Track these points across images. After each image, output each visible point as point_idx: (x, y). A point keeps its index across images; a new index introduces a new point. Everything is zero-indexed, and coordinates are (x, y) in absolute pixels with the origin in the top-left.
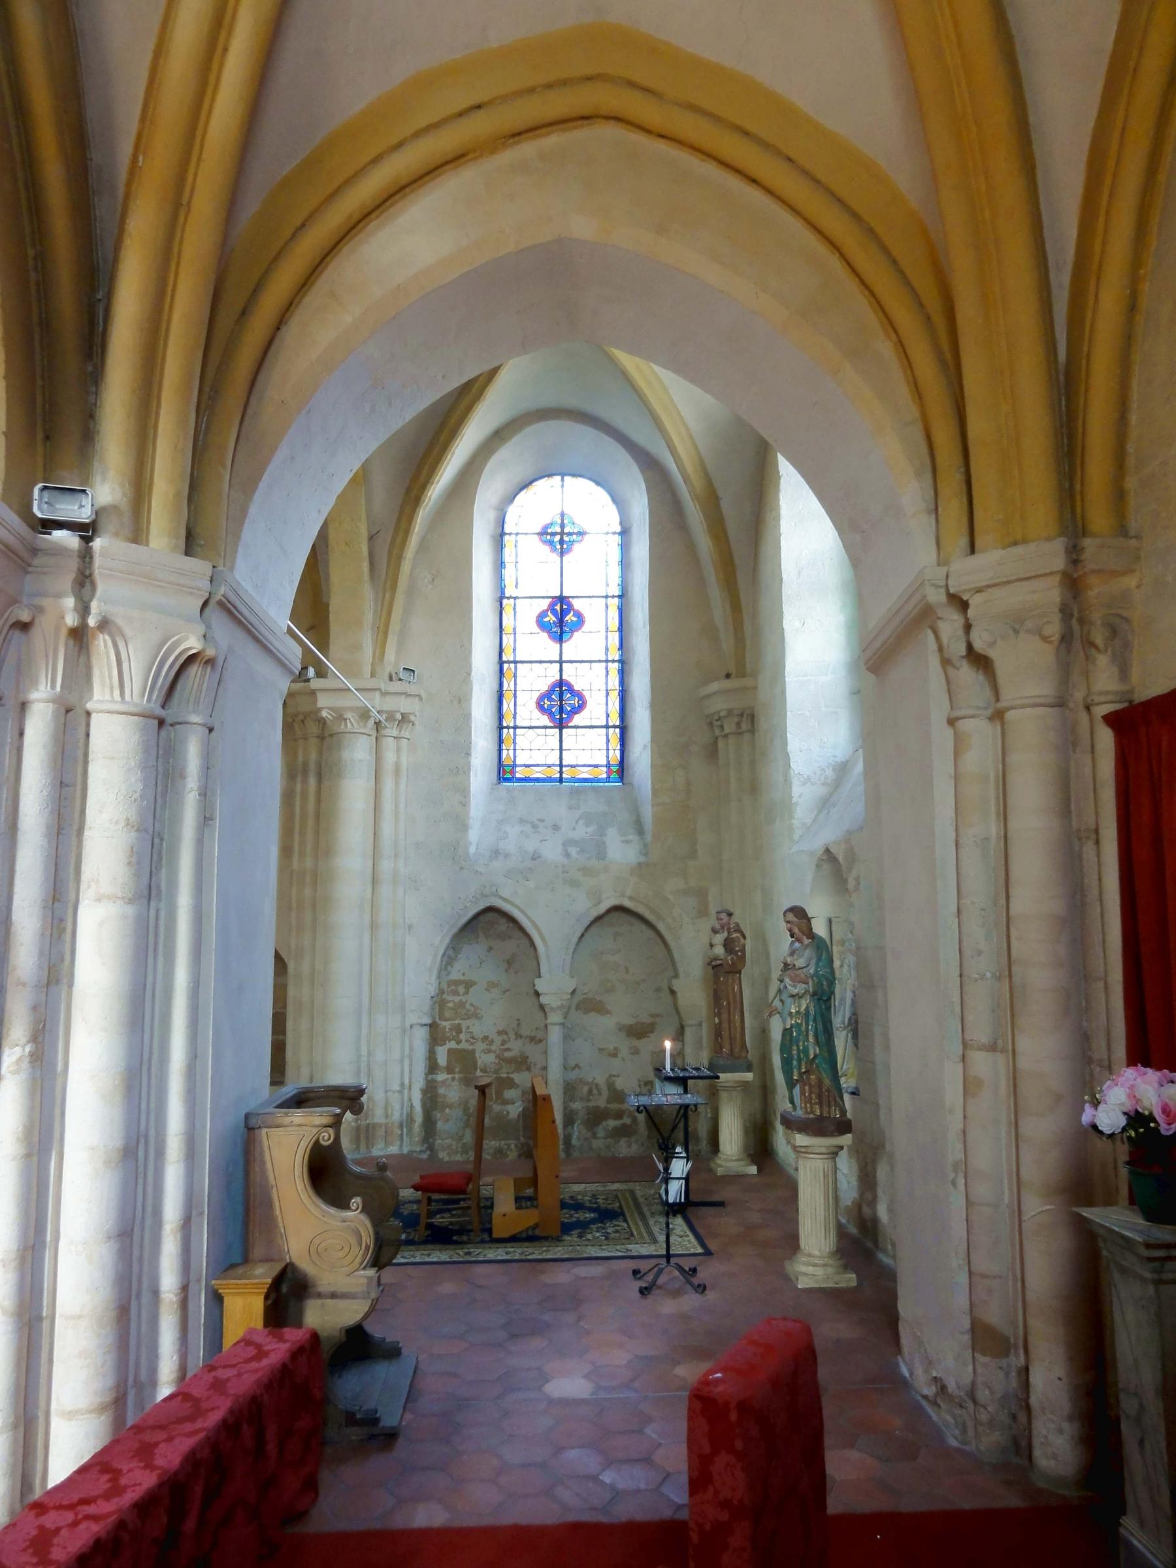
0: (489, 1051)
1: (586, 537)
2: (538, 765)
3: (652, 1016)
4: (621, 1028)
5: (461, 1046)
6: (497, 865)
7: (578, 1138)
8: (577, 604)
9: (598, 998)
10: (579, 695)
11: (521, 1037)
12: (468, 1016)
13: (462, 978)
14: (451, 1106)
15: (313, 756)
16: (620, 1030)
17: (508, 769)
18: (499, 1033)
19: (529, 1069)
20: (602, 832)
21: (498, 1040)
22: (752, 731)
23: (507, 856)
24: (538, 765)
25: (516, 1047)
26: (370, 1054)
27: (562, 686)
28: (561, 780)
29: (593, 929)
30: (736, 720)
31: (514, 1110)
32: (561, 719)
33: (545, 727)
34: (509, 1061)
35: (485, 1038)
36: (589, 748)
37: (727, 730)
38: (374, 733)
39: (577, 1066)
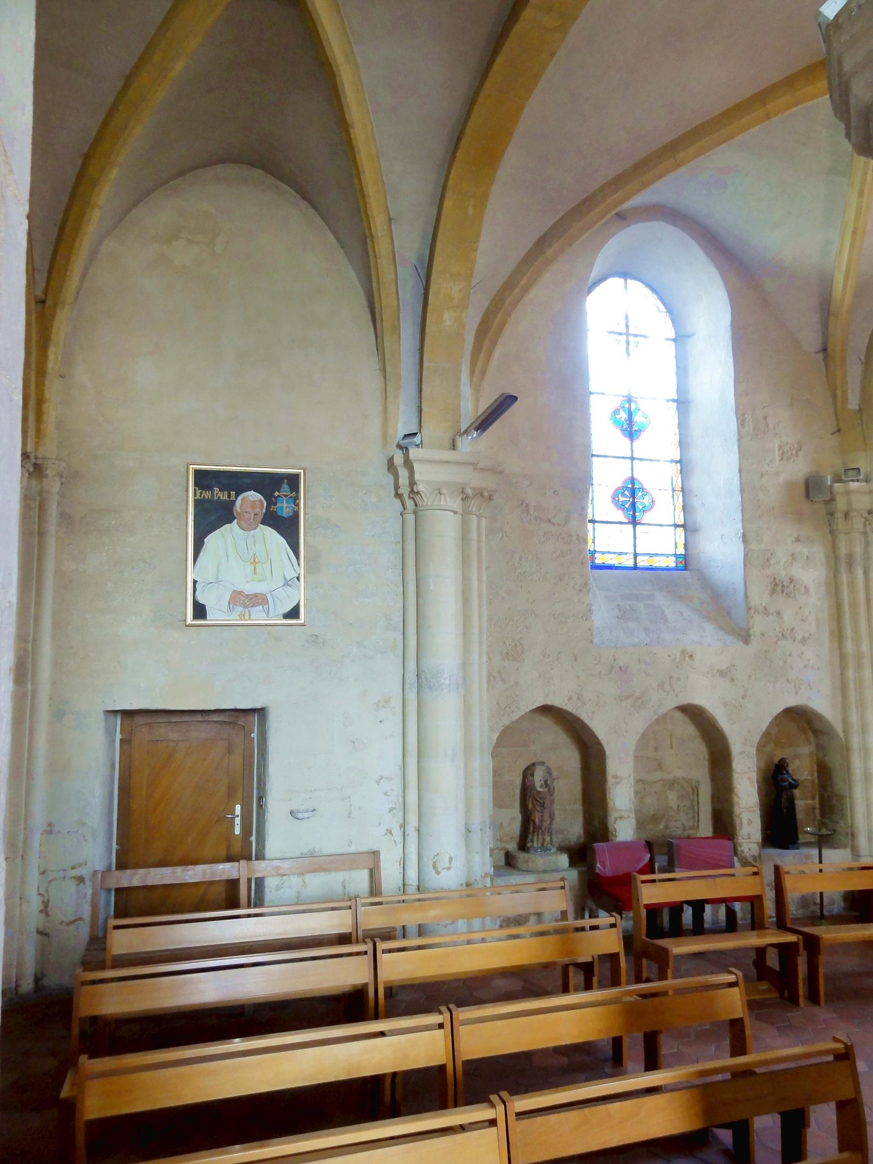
15: (858, 550)
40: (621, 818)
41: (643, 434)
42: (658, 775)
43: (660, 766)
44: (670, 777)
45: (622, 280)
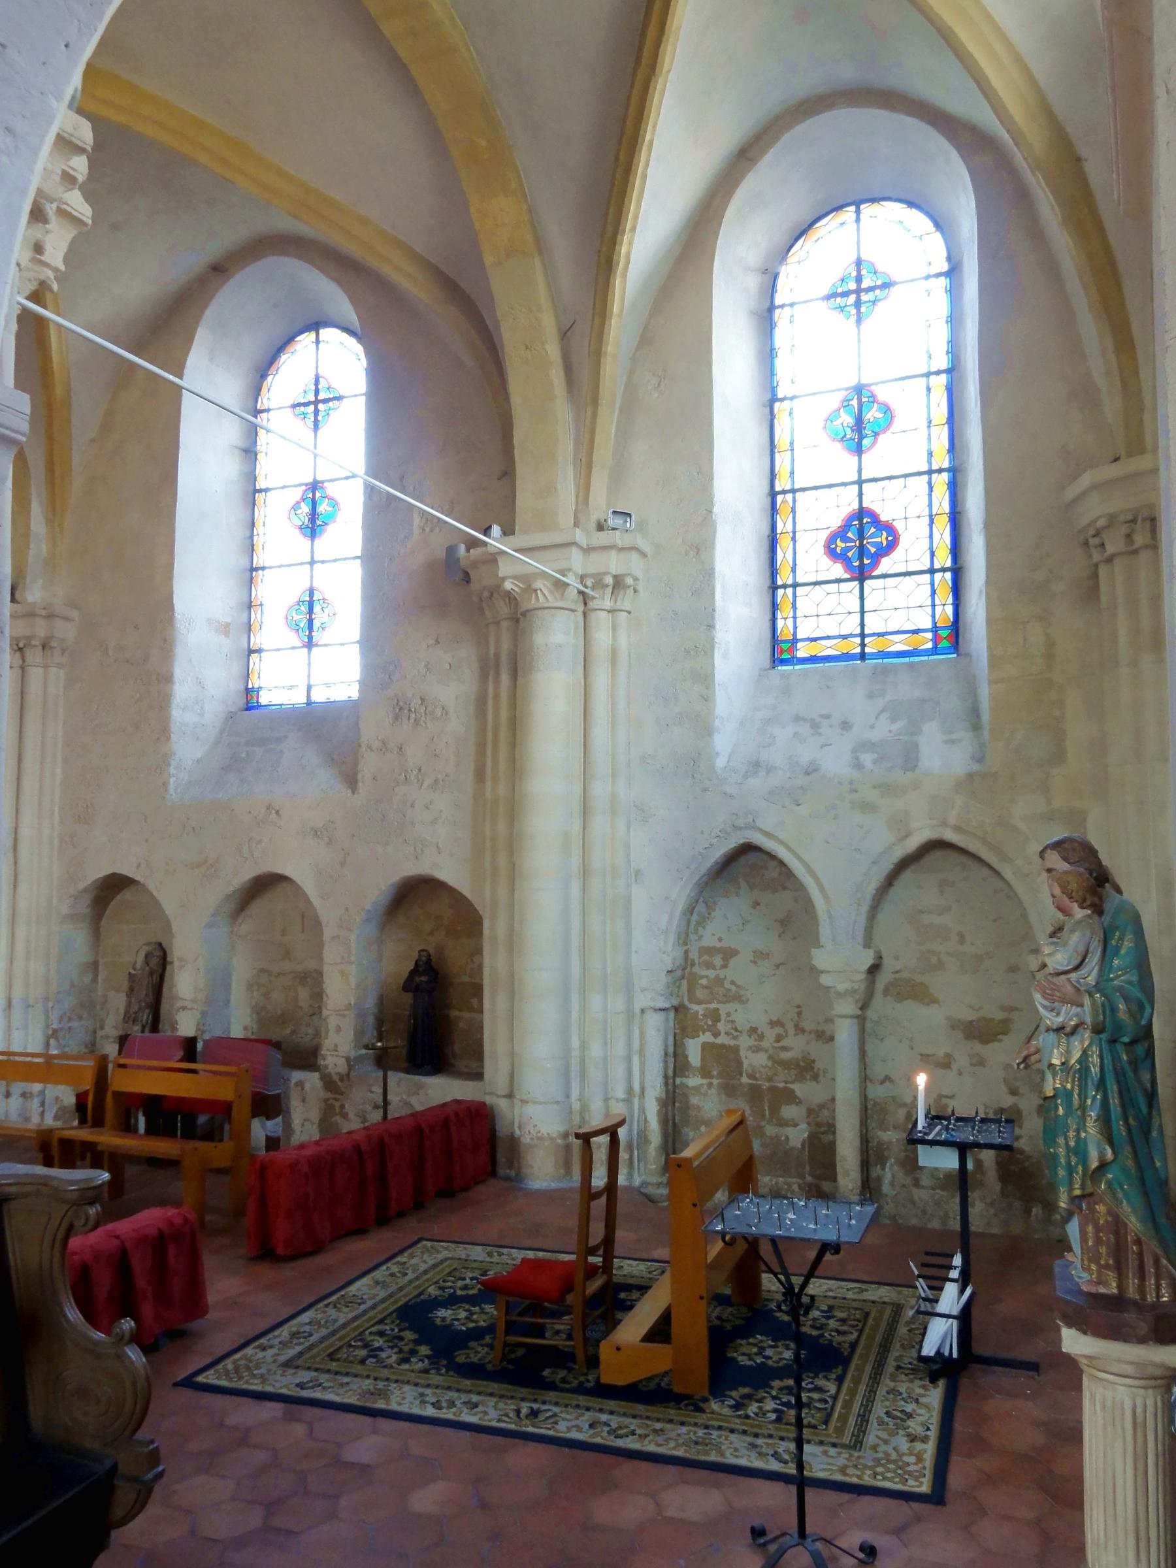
0: (758, 1049)
1: (894, 290)
2: (828, 638)
3: (1003, 1008)
4: (954, 1025)
5: (719, 1041)
6: (755, 783)
7: (892, 1184)
8: (882, 394)
9: (919, 978)
10: (889, 528)
11: (803, 1031)
12: (729, 998)
13: (719, 945)
14: (708, 1123)
15: (505, 645)
16: (953, 1027)
17: (785, 646)
18: (773, 1024)
19: (815, 1078)
20: (914, 728)
21: (771, 1034)
22: (1154, 546)
23: (770, 770)
24: (828, 638)
25: (796, 1046)
26: (583, 1046)
27: (863, 518)
28: (863, 656)
29: (907, 875)
30: (1124, 529)
31: (797, 1136)
32: (862, 564)
33: (838, 581)
34: (786, 1064)
35: (753, 1030)
36: (904, 605)
37: (1110, 549)
38: (581, 608)
39: (887, 1079)
40: (184, 1008)
41: (330, 528)
42: (288, 966)
43: (288, 955)
44: (299, 968)
45: (313, 335)
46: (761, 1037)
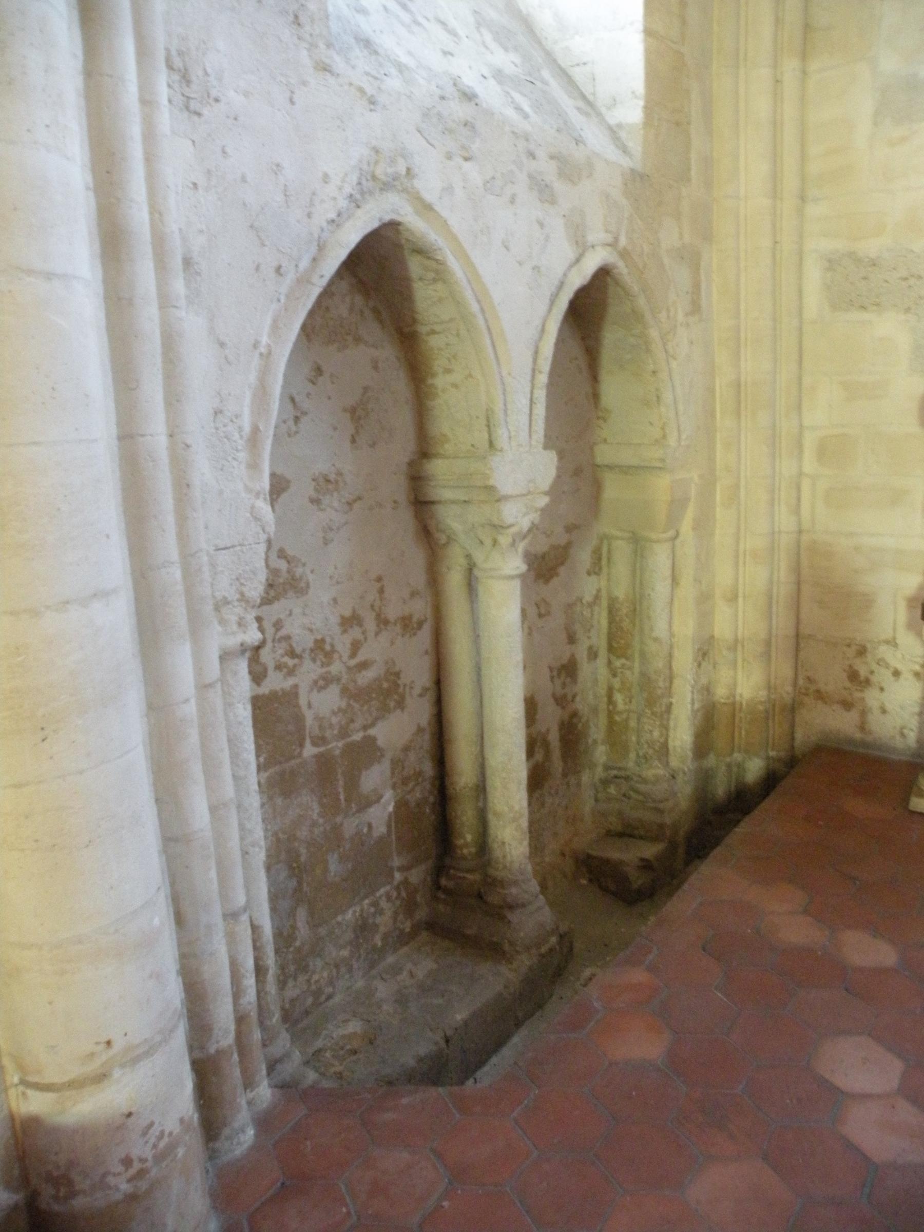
11: (386, 622)
21: (343, 644)
46: (329, 655)
